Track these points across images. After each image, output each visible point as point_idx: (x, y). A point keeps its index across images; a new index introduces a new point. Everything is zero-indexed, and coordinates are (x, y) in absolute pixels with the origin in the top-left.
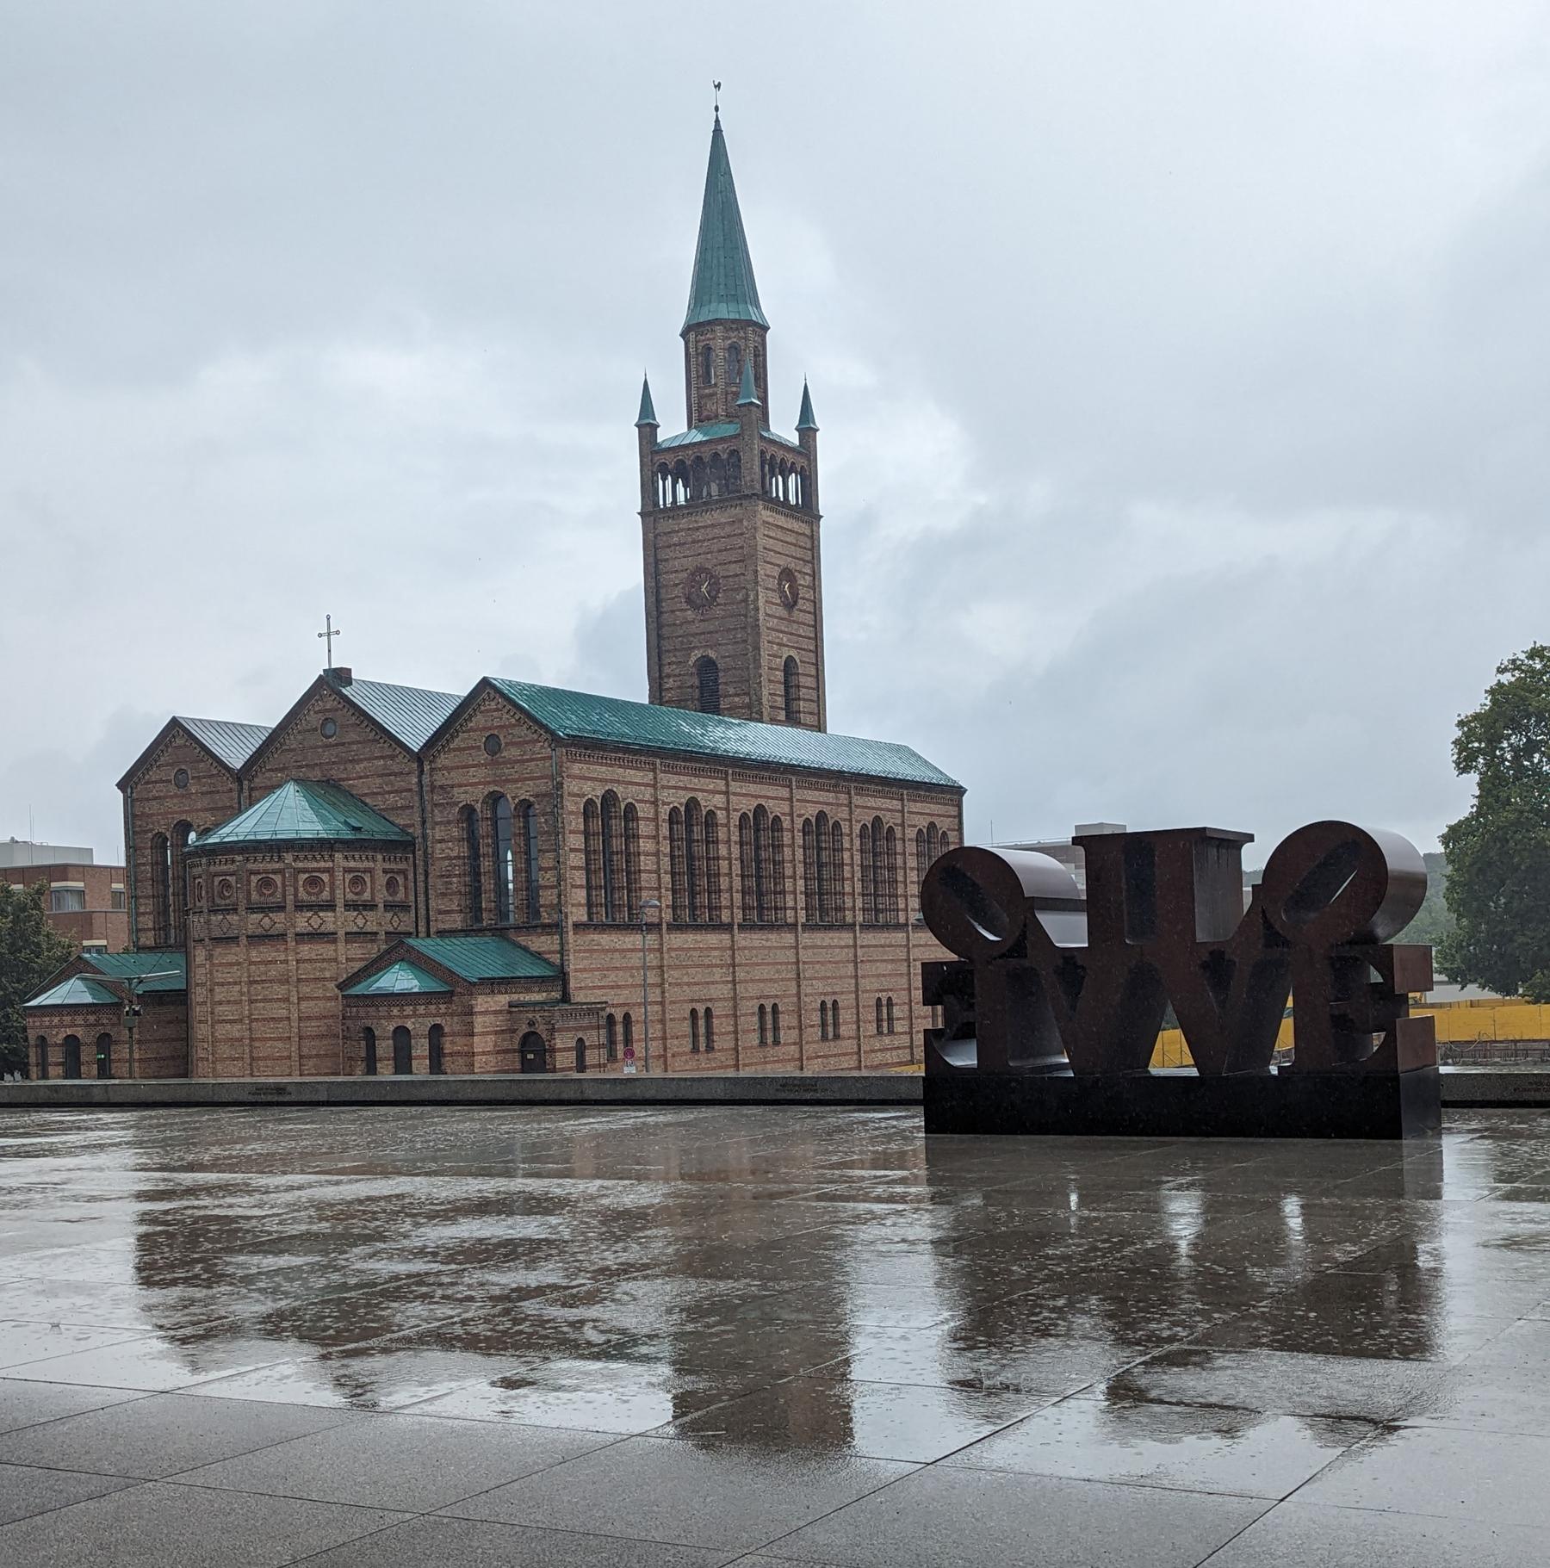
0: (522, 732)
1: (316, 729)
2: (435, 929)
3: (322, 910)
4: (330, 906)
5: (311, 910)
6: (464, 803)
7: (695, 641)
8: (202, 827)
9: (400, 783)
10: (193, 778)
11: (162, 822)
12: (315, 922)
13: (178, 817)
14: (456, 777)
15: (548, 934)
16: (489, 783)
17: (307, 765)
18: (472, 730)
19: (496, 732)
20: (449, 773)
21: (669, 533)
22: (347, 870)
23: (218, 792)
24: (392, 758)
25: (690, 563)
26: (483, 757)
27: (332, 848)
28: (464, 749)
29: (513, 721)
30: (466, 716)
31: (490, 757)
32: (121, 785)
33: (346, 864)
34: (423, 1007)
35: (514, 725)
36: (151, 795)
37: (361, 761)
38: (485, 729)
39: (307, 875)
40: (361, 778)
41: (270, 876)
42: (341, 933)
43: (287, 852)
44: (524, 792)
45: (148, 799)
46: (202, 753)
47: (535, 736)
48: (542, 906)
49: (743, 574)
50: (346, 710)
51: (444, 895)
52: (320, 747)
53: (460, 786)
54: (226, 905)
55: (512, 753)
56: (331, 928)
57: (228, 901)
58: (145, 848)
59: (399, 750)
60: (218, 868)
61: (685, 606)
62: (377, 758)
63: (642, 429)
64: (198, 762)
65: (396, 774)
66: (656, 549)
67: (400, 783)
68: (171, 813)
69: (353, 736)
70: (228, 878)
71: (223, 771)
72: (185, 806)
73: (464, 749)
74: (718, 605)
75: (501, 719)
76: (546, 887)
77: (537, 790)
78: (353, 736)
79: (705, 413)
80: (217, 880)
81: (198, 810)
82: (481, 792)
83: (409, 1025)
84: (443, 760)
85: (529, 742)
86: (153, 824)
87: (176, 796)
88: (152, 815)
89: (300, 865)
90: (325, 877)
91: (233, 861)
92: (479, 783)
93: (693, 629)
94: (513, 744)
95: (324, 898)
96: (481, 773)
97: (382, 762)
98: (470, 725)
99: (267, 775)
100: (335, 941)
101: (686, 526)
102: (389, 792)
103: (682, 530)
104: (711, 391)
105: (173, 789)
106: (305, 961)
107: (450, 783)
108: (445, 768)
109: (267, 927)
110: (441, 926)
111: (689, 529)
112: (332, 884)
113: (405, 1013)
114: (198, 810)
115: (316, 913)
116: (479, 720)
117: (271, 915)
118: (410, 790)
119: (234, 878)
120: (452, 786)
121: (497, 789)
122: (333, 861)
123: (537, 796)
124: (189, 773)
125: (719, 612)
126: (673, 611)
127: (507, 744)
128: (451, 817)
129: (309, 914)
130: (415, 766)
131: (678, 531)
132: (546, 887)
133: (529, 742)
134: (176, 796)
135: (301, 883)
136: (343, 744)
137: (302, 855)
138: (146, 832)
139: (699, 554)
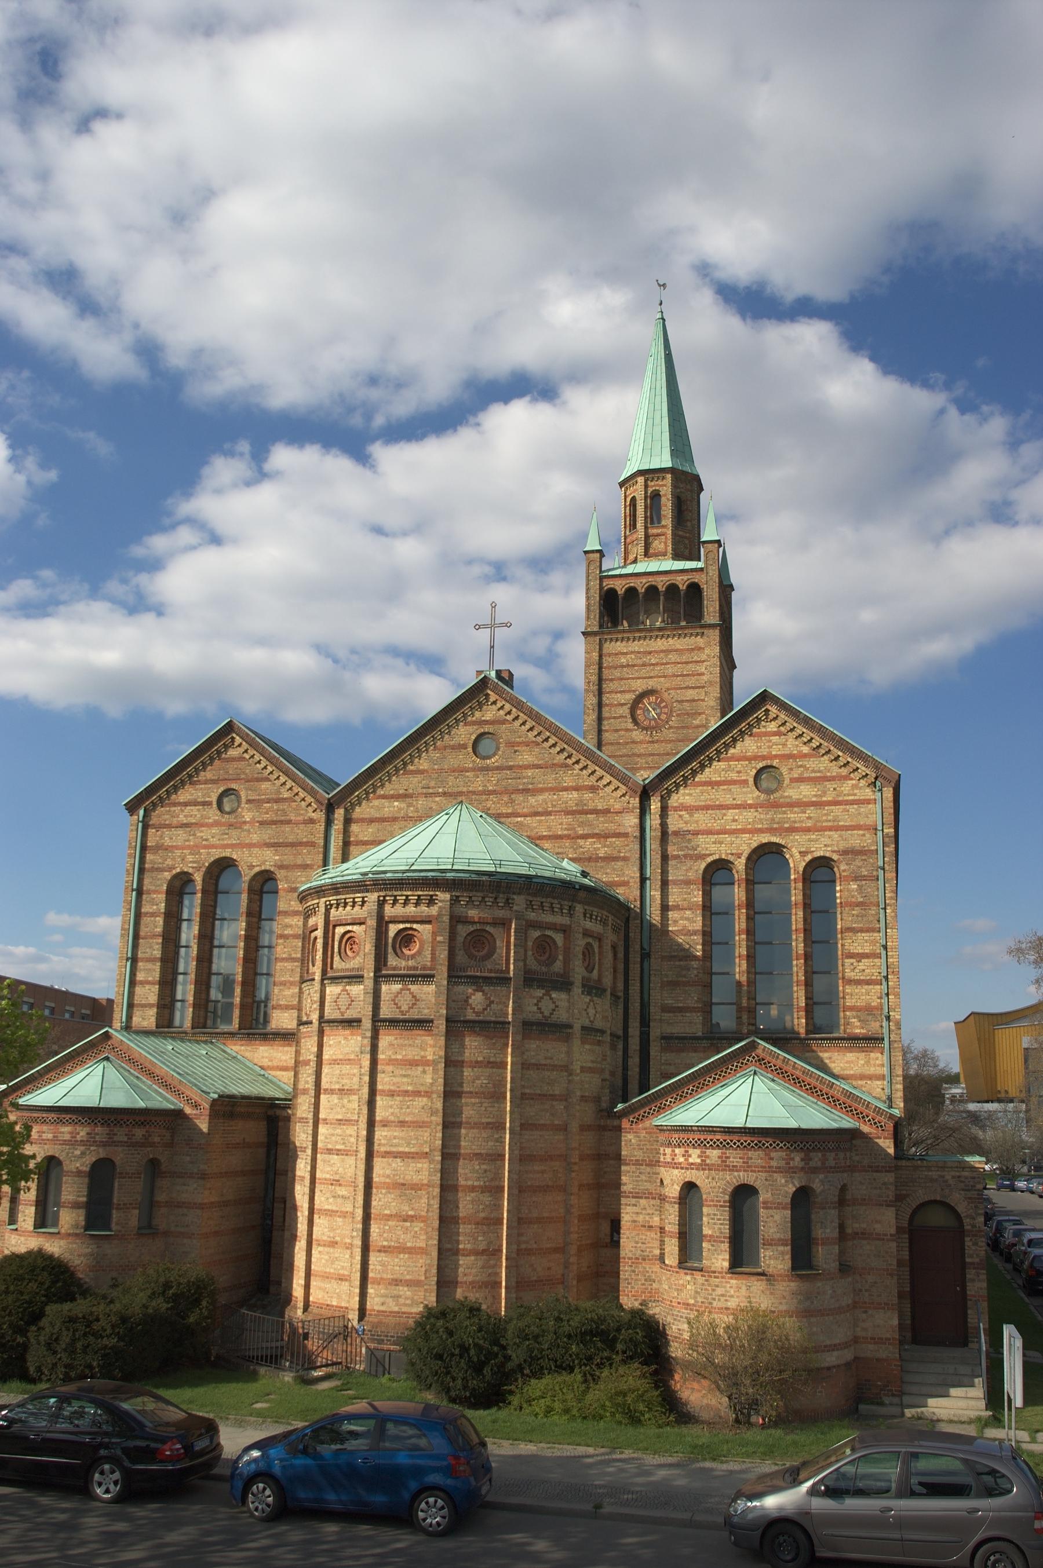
0: (822, 764)
1: (464, 746)
2: (658, 1034)
3: (555, 988)
4: (563, 984)
5: (543, 987)
6: (717, 857)
7: (642, 761)
8: (257, 869)
9: (601, 824)
10: (249, 801)
11: (190, 858)
12: (547, 1006)
13: (217, 854)
14: (703, 820)
15: (862, 1050)
16: (761, 831)
17: (444, 794)
18: (734, 758)
19: (775, 763)
20: (691, 816)
21: (616, 654)
22: (587, 933)
23: (289, 822)
24: (593, 789)
25: (640, 686)
26: (751, 795)
27: (574, 899)
28: (718, 783)
29: (805, 749)
30: (727, 738)
31: (763, 796)
32: (132, 807)
33: (589, 925)
34: (833, 1154)
35: (805, 756)
36: (175, 821)
37: (542, 791)
38: (756, 758)
39: (537, 934)
40: (536, 814)
41: (488, 928)
42: (577, 1027)
43: (519, 894)
44: (822, 846)
45: (169, 826)
46: (270, 769)
47: (844, 771)
48: (852, 1008)
49: (703, 700)
50: (517, 723)
51: (674, 984)
52: (473, 769)
53: (709, 832)
54: (409, 968)
55: (806, 792)
56: (562, 1016)
57: (411, 963)
58: (156, 892)
59: (608, 778)
60: (399, 910)
61: (630, 726)
62: (566, 789)
63: (591, 555)
64: (258, 780)
65: (596, 812)
66: (600, 668)
67: (601, 824)
68: (206, 847)
69: (526, 757)
70: (415, 926)
71: (302, 794)
72: (230, 838)
73: (718, 783)
74: (671, 727)
75: (784, 745)
76: (859, 982)
77: (843, 845)
78: (526, 757)
79: (651, 551)
80: (393, 929)
81: (250, 846)
82: (746, 844)
83: (817, 1186)
84: (683, 797)
85: (832, 779)
86: (173, 859)
87: (216, 824)
88: (177, 847)
89: (532, 916)
90: (559, 938)
91: (431, 902)
92: (743, 831)
93: (641, 749)
94: (801, 780)
95: (556, 970)
96: (749, 816)
97: (575, 794)
98: (732, 751)
99: (376, 802)
100: (568, 1039)
101: (637, 649)
102: (585, 837)
103: (632, 653)
104: (659, 531)
105: (213, 814)
106: (538, 1066)
107: (692, 827)
108: (683, 807)
109: (479, 1008)
110: (669, 1030)
111: (639, 652)
112: (567, 950)
113: (812, 1164)
114: (250, 846)
115: (547, 994)
116: (748, 745)
117: (486, 988)
118: (626, 835)
119: (428, 927)
120: (696, 833)
121: (775, 839)
122: (571, 916)
123: (845, 852)
124: (243, 794)
125: (668, 734)
126: (617, 731)
127: (793, 780)
128: (691, 875)
129: (539, 993)
130: (635, 802)
131: (626, 654)
132: (859, 982)
133: (832, 779)
134: (216, 824)
135: (530, 944)
136: (510, 768)
137: (537, 901)
138: (162, 870)
139: (651, 677)
